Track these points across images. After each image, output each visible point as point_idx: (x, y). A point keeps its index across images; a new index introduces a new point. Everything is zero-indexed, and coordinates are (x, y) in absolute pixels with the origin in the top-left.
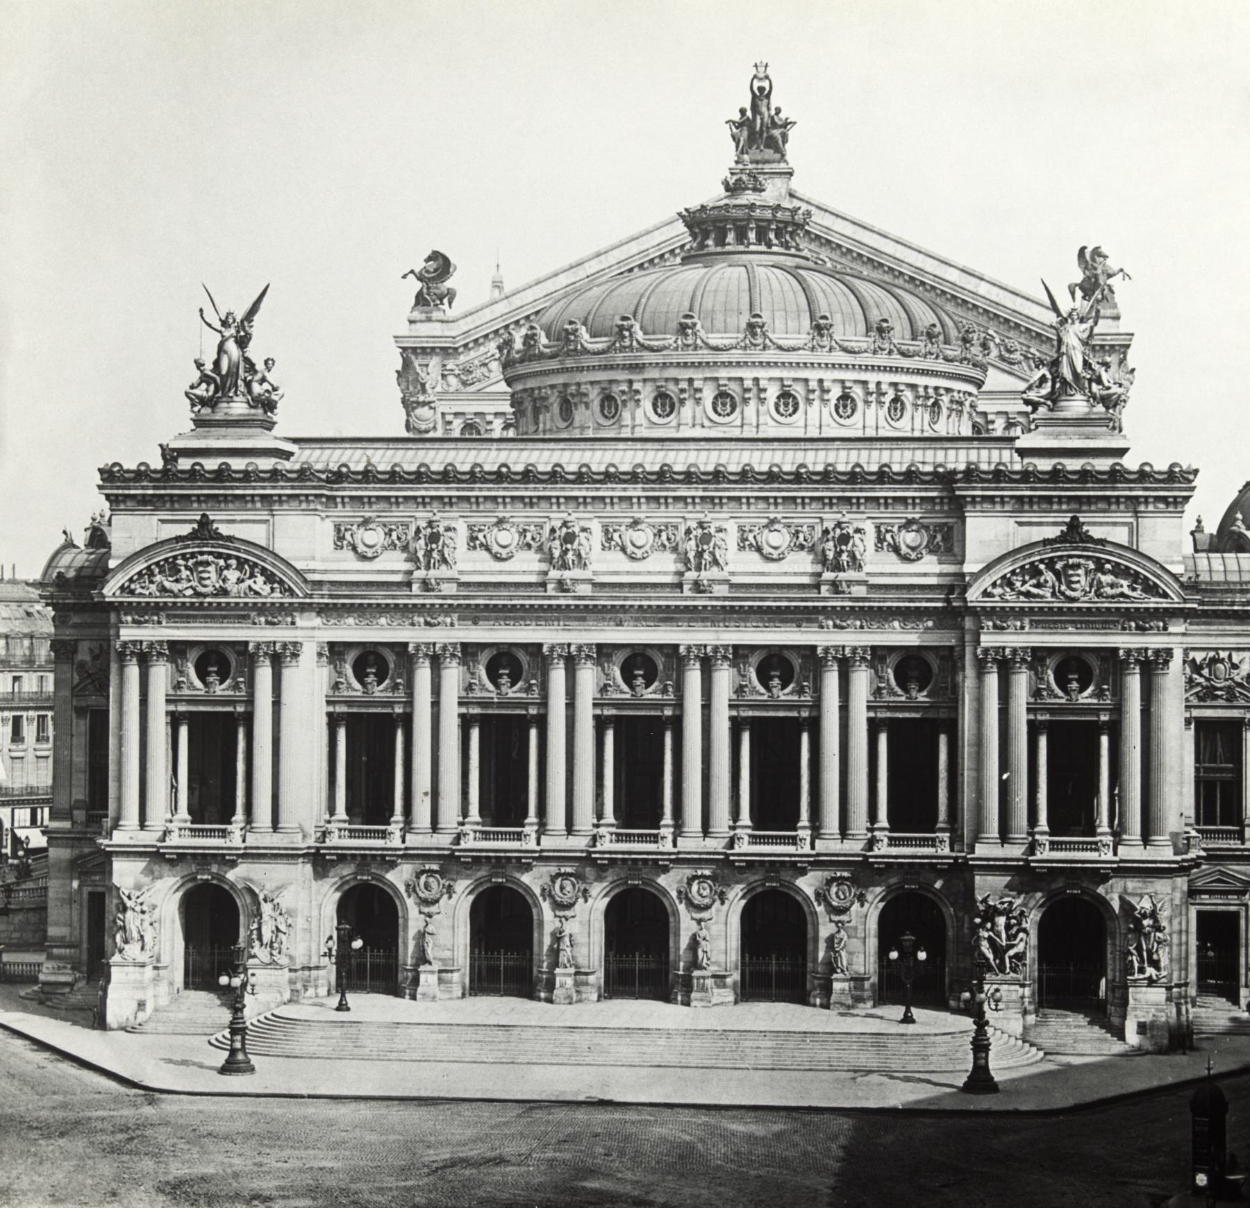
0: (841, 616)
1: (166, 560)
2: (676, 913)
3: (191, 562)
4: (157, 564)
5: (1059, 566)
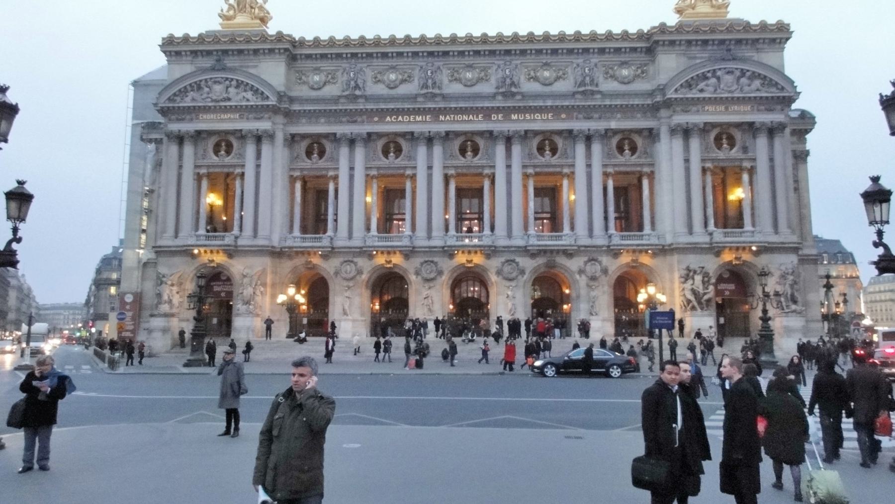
0: (588, 112)
1: (196, 83)
3: (210, 83)
4: (190, 85)
5: (719, 73)
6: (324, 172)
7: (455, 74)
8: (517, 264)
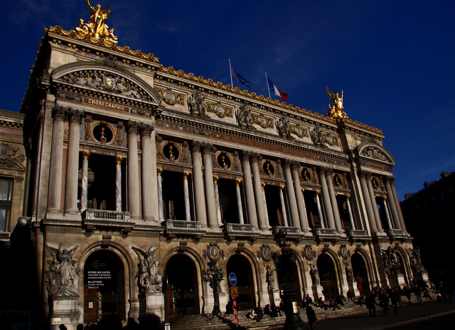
1: (88, 71)
2: (301, 264)
3: (102, 74)
4: (83, 71)
6: (179, 170)
7: (256, 118)
8: (311, 248)
